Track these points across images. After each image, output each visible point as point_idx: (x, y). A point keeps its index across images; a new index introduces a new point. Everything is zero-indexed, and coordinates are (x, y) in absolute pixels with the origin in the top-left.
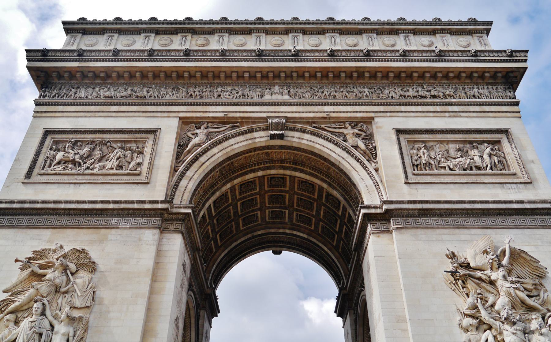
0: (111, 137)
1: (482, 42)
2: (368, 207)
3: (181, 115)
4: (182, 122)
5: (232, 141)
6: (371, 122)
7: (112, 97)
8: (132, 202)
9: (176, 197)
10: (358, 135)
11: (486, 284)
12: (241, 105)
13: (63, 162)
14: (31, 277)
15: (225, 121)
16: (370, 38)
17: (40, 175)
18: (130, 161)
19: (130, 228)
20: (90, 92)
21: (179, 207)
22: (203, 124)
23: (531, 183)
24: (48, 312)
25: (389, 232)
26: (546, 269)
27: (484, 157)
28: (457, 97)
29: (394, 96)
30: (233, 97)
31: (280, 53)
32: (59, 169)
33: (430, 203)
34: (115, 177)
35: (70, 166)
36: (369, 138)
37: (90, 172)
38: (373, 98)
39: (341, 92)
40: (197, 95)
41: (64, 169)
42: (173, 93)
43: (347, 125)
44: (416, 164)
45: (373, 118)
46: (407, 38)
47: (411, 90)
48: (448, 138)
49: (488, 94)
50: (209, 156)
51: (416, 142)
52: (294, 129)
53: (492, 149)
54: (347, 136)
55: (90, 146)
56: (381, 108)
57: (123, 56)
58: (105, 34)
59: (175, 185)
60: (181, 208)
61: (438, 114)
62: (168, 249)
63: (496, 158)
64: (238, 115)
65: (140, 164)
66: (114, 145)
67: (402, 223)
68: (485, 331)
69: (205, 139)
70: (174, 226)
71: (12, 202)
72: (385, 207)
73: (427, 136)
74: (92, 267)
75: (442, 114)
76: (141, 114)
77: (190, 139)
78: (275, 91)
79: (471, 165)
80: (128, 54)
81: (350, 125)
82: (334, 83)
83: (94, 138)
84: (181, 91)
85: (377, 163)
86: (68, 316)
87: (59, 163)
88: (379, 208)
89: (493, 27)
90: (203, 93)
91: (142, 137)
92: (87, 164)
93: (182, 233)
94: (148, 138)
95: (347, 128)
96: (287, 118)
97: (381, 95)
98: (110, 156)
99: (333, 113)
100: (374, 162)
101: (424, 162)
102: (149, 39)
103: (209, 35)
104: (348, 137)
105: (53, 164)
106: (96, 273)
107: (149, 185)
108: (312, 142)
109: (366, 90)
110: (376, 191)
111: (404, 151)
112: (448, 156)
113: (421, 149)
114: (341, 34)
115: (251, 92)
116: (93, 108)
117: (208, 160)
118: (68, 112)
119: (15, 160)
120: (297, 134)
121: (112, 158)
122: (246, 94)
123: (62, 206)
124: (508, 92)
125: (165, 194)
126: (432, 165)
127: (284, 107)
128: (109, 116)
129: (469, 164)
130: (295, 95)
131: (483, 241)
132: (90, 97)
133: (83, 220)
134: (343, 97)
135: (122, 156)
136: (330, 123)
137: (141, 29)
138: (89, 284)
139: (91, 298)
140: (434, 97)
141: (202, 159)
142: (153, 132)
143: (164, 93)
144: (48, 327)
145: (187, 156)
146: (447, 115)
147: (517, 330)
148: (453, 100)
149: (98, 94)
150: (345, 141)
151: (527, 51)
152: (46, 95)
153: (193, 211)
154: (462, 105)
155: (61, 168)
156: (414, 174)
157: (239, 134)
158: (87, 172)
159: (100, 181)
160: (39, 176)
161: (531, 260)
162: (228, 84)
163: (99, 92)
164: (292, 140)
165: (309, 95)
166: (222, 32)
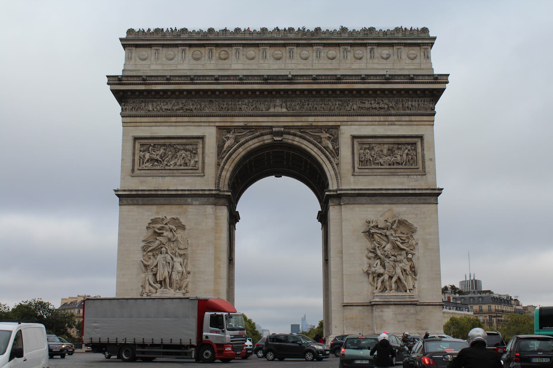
0: (176, 142)
1: (426, 55)
2: (330, 191)
3: (217, 124)
4: (218, 128)
5: (250, 143)
6: (338, 128)
7: (170, 110)
8: (198, 190)
9: (220, 183)
10: (329, 138)
11: (383, 236)
12: (255, 116)
13: (150, 160)
14: (154, 234)
15: (245, 128)
16: (345, 51)
17: (140, 170)
18: (190, 159)
19: (199, 205)
20: (155, 106)
21: (224, 191)
22: (231, 131)
23: (425, 175)
24: (169, 252)
25: (340, 205)
26: (417, 228)
27: (404, 156)
28: (396, 108)
29: (355, 108)
30: (249, 109)
31: (280, 77)
32: (149, 165)
33: (363, 190)
34: (184, 171)
35: (156, 163)
36: (335, 140)
37: (169, 168)
38: (341, 109)
39: (320, 104)
40: (225, 107)
41: (152, 165)
42: (209, 106)
43: (323, 131)
44: (361, 160)
45: (339, 126)
46: (372, 51)
47: (367, 102)
48: (384, 141)
49: (417, 106)
50: (237, 154)
51: (363, 144)
52: (289, 134)
53: (409, 150)
54: (322, 139)
55: (164, 147)
56: (345, 118)
57: (174, 80)
58: (152, 48)
59: (220, 175)
60: (225, 192)
61: (381, 123)
62: (220, 215)
63: (410, 157)
64: (253, 124)
65: (196, 162)
66: (178, 147)
67: (347, 202)
68: (378, 259)
69: (234, 142)
70: (222, 201)
71: (131, 191)
72: (339, 192)
73: (371, 140)
74: (183, 227)
75: (384, 123)
76: (191, 124)
77: (224, 142)
78: (277, 104)
79: (394, 162)
80: (177, 79)
81: (324, 130)
82: (316, 97)
83: (165, 142)
84: (215, 103)
85: (339, 159)
86: (179, 254)
87: (148, 161)
88: (336, 191)
89: (436, 42)
90: (229, 105)
91: (194, 141)
92: (165, 163)
93: (227, 206)
94: (199, 142)
95: (322, 133)
96: (285, 127)
97: (346, 107)
98: (178, 155)
99: (314, 123)
100: (337, 158)
101: (366, 159)
102: (185, 53)
103: (228, 48)
104: (323, 140)
105: (145, 162)
106: (186, 230)
107: (205, 177)
108: (300, 143)
109: (337, 103)
110: (335, 179)
111: (356, 152)
112: (382, 154)
113: (366, 149)
114: (324, 46)
115: (261, 106)
116: (159, 119)
117: (236, 157)
118: (144, 122)
119: (122, 160)
120: (291, 137)
121: (179, 157)
122: (258, 107)
123: (160, 193)
124: (431, 104)
125: (215, 183)
126: (371, 161)
127: (282, 118)
128: (171, 125)
129: (393, 161)
130: (290, 107)
131: (388, 212)
132: (155, 110)
133: (172, 200)
134: (322, 109)
135: (185, 156)
136: (312, 129)
137: (178, 44)
138: (184, 236)
139: (187, 244)
140: (381, 108)
141: (233, 156)
142: (202, 138)
143: (204, 106)
144: (171, 259)
145: (224, 154)
146: (387, 123)
147: (390, 261)
148: (393, 112)
149: (160, 107)
150: (319, 143)
151: (448, 75)
152: (126, 108)
153: (232, 193)
154: (398, 116)
155: (151, 165)
156: (359, 168)
157: (254, 138)
158: (167, 168)
159: (176, 175)
160: (139, 171)
161: (409, 225)
162: (245, 98)
163: (160, 106)
164: (288, 142)
165: (299, 107)
166: (237, 46)
